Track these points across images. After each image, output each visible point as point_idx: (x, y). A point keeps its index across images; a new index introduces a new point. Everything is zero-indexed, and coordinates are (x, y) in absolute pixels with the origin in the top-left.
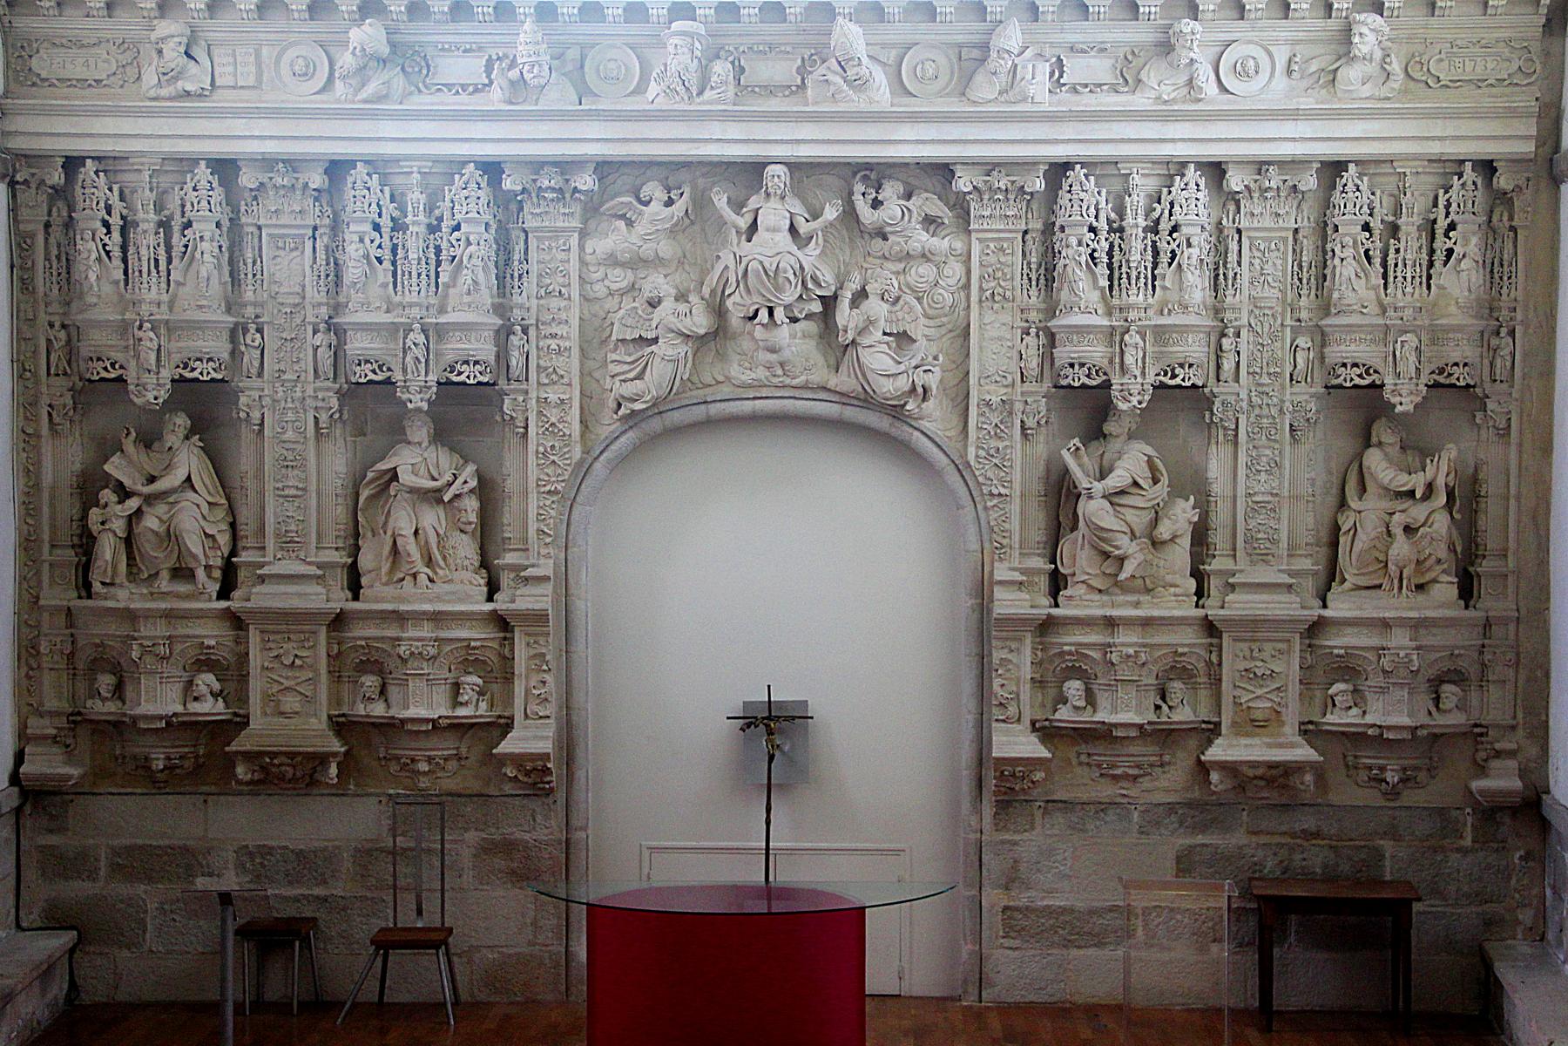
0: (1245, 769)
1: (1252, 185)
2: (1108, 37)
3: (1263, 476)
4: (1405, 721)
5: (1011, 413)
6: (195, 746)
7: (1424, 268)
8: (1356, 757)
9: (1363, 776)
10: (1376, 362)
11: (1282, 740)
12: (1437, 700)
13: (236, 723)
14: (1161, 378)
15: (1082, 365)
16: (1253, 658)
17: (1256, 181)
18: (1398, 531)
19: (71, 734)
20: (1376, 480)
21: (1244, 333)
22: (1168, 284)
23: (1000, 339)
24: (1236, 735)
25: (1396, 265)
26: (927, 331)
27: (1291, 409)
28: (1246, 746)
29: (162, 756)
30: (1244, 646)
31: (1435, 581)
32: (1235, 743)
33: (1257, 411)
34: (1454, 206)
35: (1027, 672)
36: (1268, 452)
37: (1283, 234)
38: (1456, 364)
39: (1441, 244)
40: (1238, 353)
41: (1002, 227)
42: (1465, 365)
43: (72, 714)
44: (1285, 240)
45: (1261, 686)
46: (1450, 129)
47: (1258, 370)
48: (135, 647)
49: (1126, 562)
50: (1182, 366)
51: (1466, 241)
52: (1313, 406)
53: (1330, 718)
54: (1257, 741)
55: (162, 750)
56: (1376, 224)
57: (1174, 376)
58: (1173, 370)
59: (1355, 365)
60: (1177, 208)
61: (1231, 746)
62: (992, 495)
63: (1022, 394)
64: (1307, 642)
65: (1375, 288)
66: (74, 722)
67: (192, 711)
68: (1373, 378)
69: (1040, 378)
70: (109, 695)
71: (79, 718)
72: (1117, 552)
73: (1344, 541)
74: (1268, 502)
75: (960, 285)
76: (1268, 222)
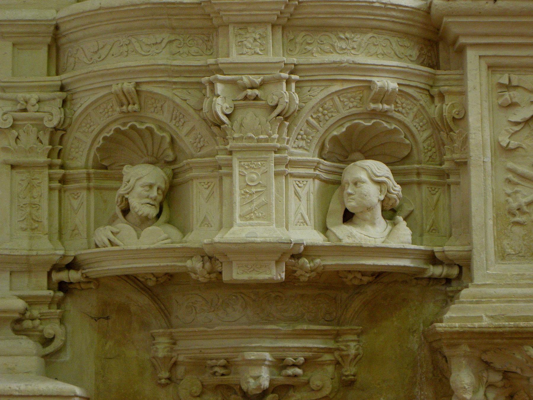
6: (337, 336)
13: (434, 280)
19: (55, 311)
29: (268, 356)
43: (57, 268)
48: (219, 88)
55: (267, 343)
66: (63, 286)
67: (347, 241)
70: (153, 212)
71: (74, 276)
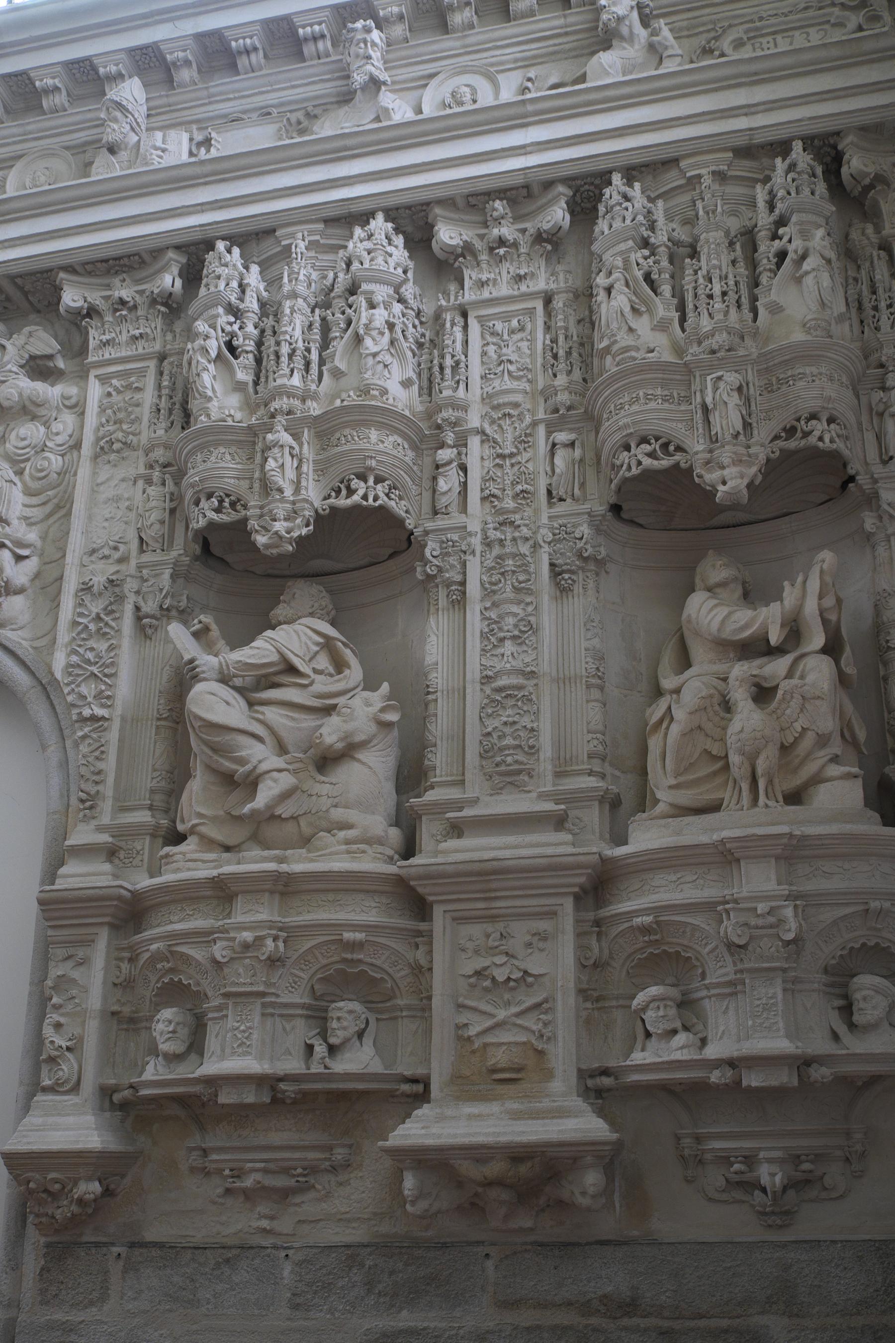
0: (467, 1168)
1: (478, 245)
2: (272, 98)
3: (509, 647)
4: (781, 1045)
5: (120, 599)
7: (743, 287)
8: (698, 1139)
9: (715, 1178)
10: (677, 430)
11: (546, 1103)
12: (847, 1010)
14: (332, 500)
15: (209, 496)
16: (493, 951)
17: (482, 237)
18: (741, 696)
20: (697, 634)
21: (474, 442)
22: (340, 363)
23: (117, 499)
24: (458, 1098)
25: (695, 288)
26: (28, 512)
27: (550, 537)
28: (470, 1117)
30: (475, 930)
31: (817, 780)
32: (449, 1112)
33: (496, 550)
34: (781, 193)
35: (95, 1000)
36: (515, 609)
37: (529, 305)
38: (813, 416)
39: (767, 249)
40: (464, 468)
41: (129, 353)
42: (831, 420)
44: (531, 312)
45: (508, 1004)
46: (761, 94)
47: (496, 492)
49: (261, 786)
50: (363, 477)
51: (805, 235)
52: (585, 530)
53: (638, 1057)
54: (495, 1108)
56: (660, 238)
57: (351, 492)
58: (348, 488)
59: (644, 440)
60: (356, 265)
61: (441, 1118)
62: (84, 720)
63: (140, 567)
64: (591, 916)
65: (662, 326)
68: (676, 458)
69: (167, 542)
72: (241, 770)
73: (654, 744)
74: (520, 688)
75: (71, 443)
76: (504, 290)
